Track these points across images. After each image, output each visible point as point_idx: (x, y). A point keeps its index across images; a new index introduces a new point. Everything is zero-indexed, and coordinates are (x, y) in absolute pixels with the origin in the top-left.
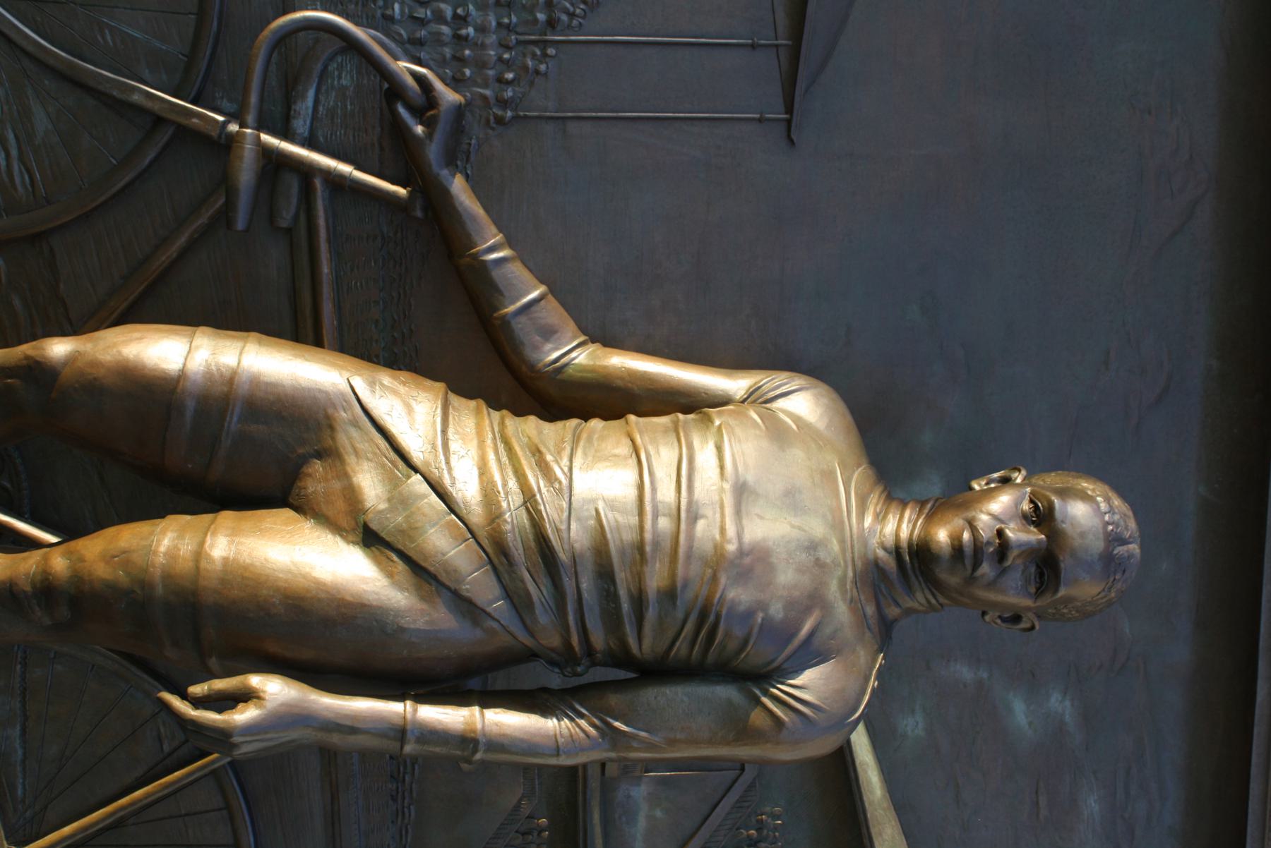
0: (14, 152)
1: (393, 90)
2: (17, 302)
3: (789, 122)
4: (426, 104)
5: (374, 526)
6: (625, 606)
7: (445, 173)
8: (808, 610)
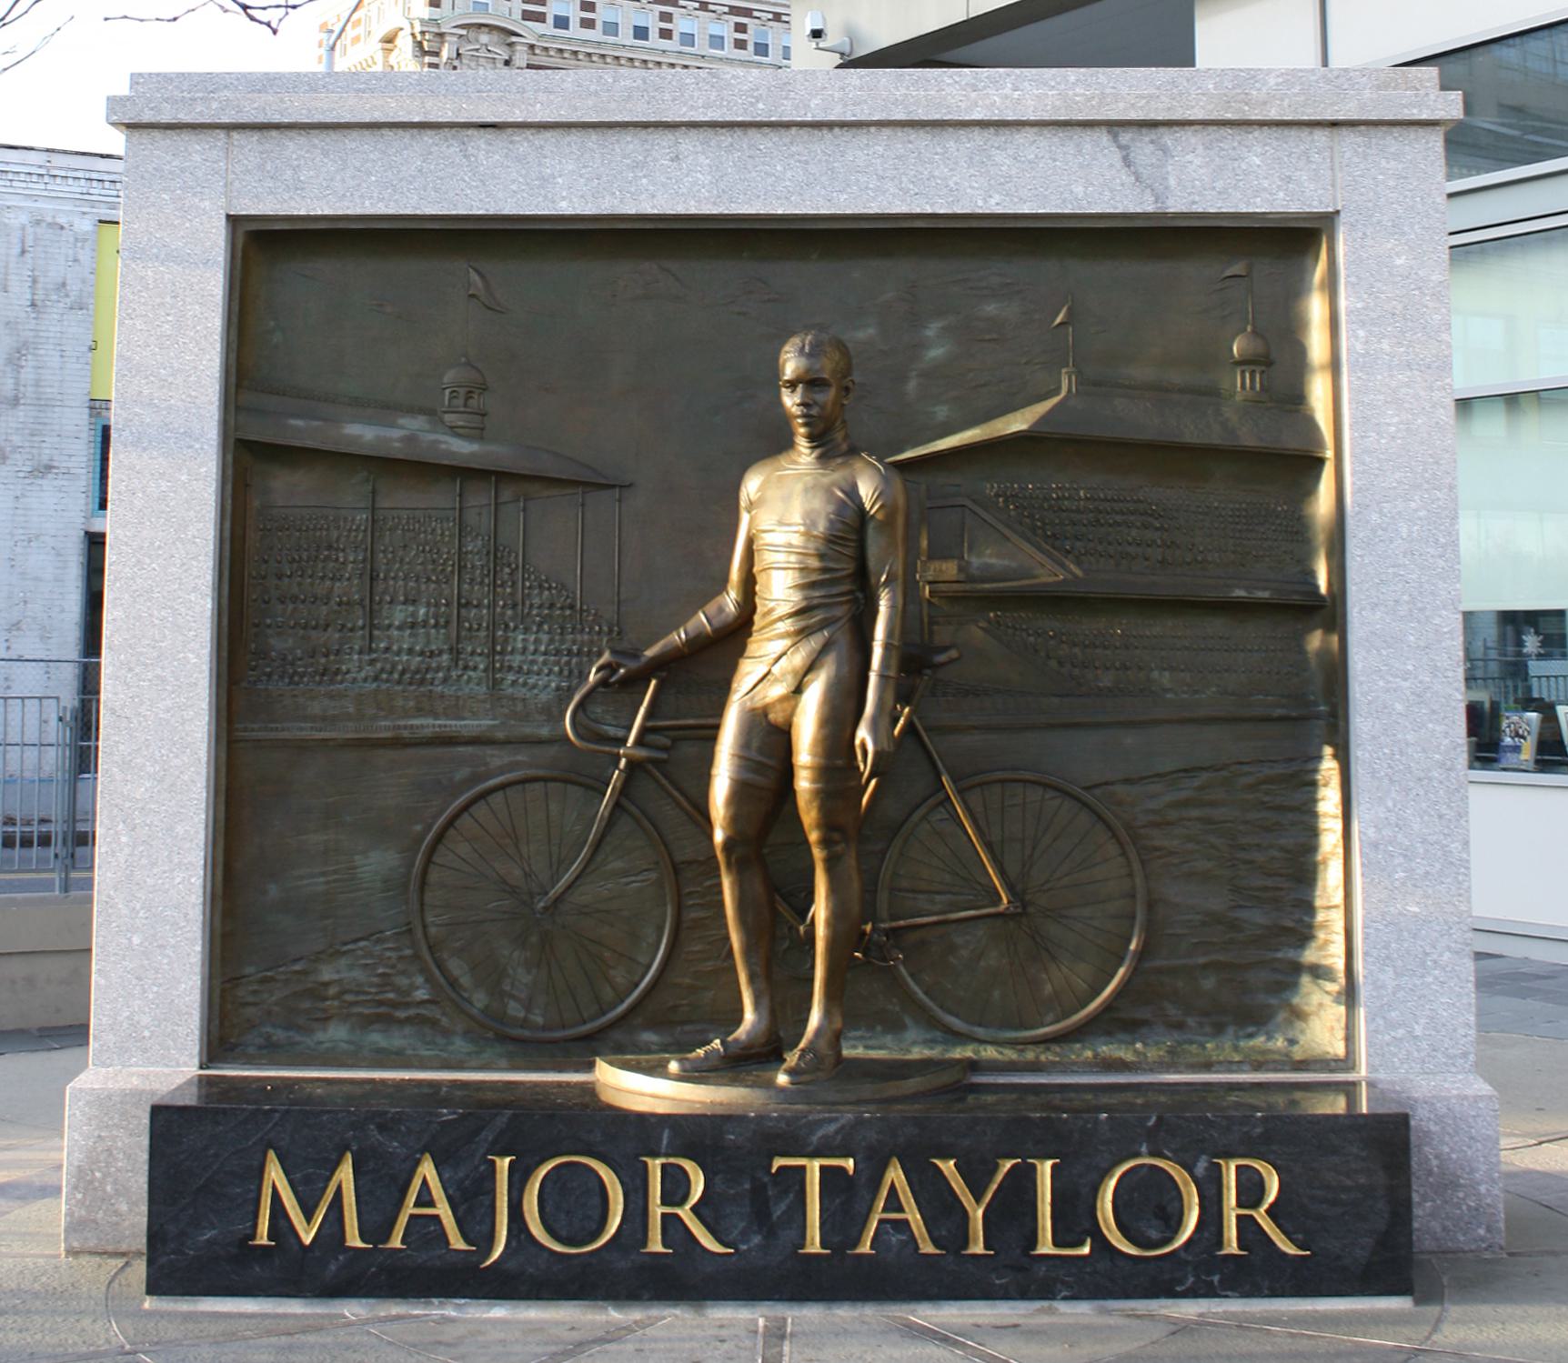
0: (633, 878)
1: (603, 683)
2: (708, 883)
3: (621, 487)
4: (609, 668)
5: (793, 688)
6: (827, 576)
7: (643, 660)
8: (833, 494)
